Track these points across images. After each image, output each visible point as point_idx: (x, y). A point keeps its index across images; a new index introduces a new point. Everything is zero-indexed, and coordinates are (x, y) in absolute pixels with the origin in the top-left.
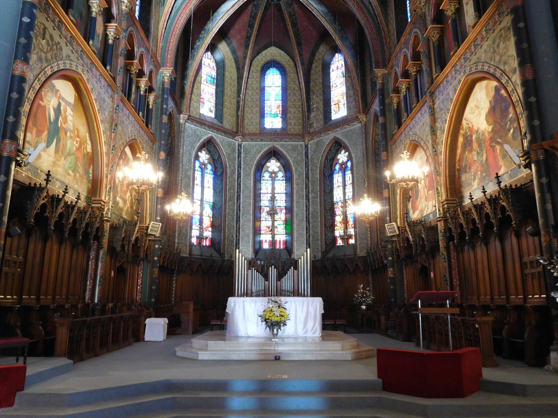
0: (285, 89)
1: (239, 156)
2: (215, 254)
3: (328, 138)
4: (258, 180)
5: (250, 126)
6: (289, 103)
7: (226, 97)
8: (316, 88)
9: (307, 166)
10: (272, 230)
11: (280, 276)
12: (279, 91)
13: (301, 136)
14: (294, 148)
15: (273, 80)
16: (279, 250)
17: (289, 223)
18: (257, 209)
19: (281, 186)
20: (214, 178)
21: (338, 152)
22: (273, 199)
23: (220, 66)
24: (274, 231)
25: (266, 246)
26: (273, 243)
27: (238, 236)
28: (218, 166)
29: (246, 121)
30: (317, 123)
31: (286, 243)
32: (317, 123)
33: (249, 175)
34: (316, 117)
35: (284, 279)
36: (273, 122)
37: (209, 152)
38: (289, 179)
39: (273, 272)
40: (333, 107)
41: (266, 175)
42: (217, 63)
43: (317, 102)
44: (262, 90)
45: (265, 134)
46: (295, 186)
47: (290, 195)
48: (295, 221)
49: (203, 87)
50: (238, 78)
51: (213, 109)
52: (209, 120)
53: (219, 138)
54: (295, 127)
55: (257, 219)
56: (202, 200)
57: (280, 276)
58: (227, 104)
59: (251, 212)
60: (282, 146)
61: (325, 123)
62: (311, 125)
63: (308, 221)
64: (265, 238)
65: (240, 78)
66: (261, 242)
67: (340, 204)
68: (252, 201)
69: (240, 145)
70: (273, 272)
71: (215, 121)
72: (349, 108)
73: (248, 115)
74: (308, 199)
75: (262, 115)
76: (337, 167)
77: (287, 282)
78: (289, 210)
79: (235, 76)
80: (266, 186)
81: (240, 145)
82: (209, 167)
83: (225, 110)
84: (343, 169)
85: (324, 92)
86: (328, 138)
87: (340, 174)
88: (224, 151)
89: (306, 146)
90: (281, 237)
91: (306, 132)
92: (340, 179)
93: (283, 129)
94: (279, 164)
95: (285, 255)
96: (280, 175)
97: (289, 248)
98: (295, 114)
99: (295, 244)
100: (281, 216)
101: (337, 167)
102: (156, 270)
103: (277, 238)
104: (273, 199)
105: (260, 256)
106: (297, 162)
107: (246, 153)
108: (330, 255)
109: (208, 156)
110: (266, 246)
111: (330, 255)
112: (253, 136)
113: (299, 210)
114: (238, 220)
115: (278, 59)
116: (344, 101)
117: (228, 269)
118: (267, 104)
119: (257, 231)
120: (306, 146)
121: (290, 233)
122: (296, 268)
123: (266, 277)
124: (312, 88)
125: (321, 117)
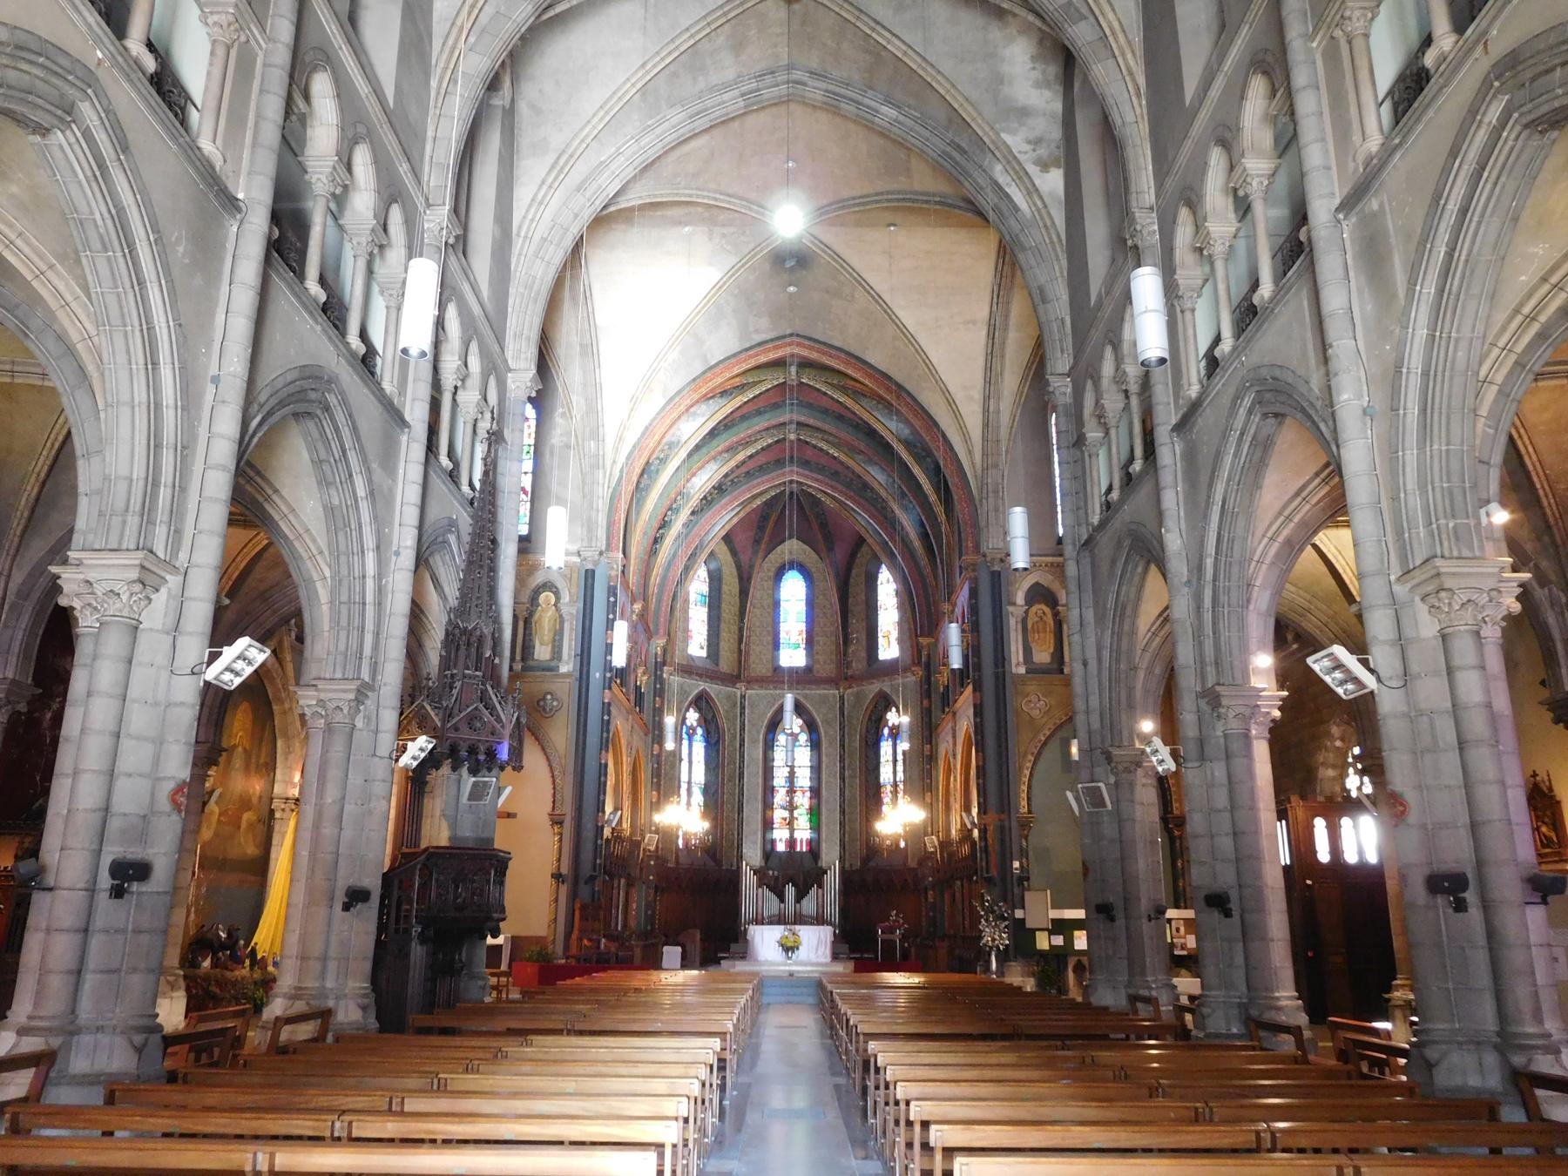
0: (811, 603)
1: (742, 714)
2: (711, 863)
3: (872, 689)
4: (769, 746)
5: (758, 667)
6: (817, 629)
7: (723, 625)
8: (857, 608)
9: (842, 728)
10: (790, 823)
11: (799, 897)
12: (801, 607)
13: (833, 682)
14: (824, 700)
15: (793, 590)
16: (801, 853)
17: (815, 812)
18: (769, 790)
19: (803, 756)
20: (706, 748)
21: (887, 709)
22: (791, 777)
23: (715, 579)
24: (793, 828)
25: (781, 847)
26: (791, 842)
27: (740, 834)
28: (712, 730)
29: (752, 658)
30: (858, 665)
31: (810, 842)
32: (858, 665)
33: (757, 741)
34: (857, 649)
35: (805, 902)
36: (793, 656)
37: (699, 710)
38: (815, 745)
39: (790, 891)
40: (881, 641)
41: (782, 739)
42: (709, 572)
43: (858, 635)
44: (776, 604)
45: (779, 677)
46: (824, 758)
47: (816, 769)
48: (824, 810)
49: (691, 613)
50: (741, 592)
51: (705, 644)
52: (699, 664)
53: (713, 689)
54: (827, 668)
55: (768, 805)
56: (689, 783)
57: (799, 899)
58: (724, 635)
59: (760, 797)
60: (806, 696)
61: (869, 665)
62: (849, 665)
63: (843, 812)
64: (780, 835)
65: (744, 593)
66: (773, 842)
67: (889, 788)
68: (760, 781)
69: (743, 697)
70: (790, 891)
71: (710, 665)
72: (901, 649)
73: (755, 649)
74: (842, 778)
75: (776, 645)
76: (886, 731)
77: (809, 905)
78: (816, 792)
79: (736, 589)
80: (779, 756)
81: (743, 697)
82: (700, 731)
83: (722, 644)
84: (895, 734)
85: (867, 616)
86: (872, 689)
87: (890, 742)
88: (721, 707)
89: (842, 698)
90: (803, 833)
91: (843, 677)
92: (890, 751)
93: (808, 669)
94: (800, 721)
95: (808, 863)
96: (803, 738)
97: (814, 849)
98: (826, 644)
99: (824, 846)
100: (803, 801)
101: (886, 731)
102: (652, 891)
103: (797, 835)
104: (791, 777)
105: (774, 861)
106: (827, 722)
107: (751, 706)
108: (872, 864)
109: (697, 715)
110: (781, 847)
111: (872, 864)
112: (761, 681)
113: (831, 795)
114: (740, 810)
115: (801, 558)
116: (895, 634)
117: (732, 883)
118: (783, 628)
119: (768, 825)
120: (842, 698)
121: (816, 827)
122: (820, 886)
123: (782, 899)
124: (851, 607)
125: (864, 654)
